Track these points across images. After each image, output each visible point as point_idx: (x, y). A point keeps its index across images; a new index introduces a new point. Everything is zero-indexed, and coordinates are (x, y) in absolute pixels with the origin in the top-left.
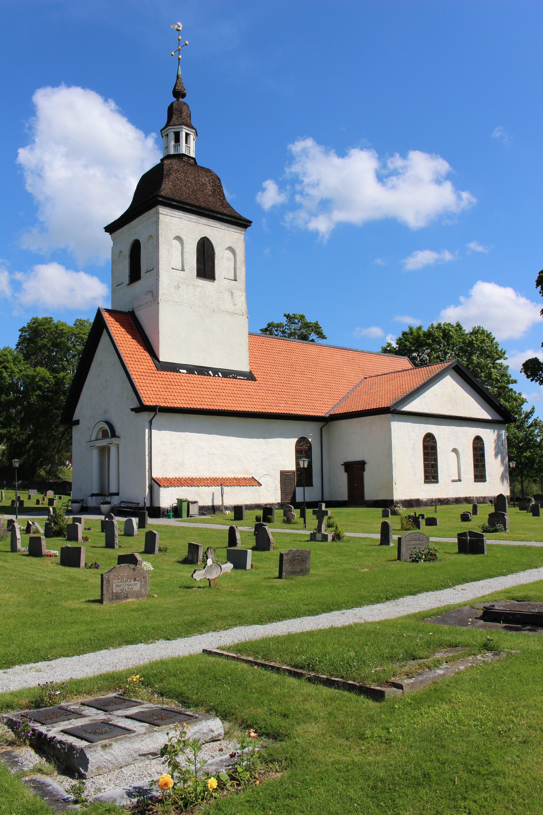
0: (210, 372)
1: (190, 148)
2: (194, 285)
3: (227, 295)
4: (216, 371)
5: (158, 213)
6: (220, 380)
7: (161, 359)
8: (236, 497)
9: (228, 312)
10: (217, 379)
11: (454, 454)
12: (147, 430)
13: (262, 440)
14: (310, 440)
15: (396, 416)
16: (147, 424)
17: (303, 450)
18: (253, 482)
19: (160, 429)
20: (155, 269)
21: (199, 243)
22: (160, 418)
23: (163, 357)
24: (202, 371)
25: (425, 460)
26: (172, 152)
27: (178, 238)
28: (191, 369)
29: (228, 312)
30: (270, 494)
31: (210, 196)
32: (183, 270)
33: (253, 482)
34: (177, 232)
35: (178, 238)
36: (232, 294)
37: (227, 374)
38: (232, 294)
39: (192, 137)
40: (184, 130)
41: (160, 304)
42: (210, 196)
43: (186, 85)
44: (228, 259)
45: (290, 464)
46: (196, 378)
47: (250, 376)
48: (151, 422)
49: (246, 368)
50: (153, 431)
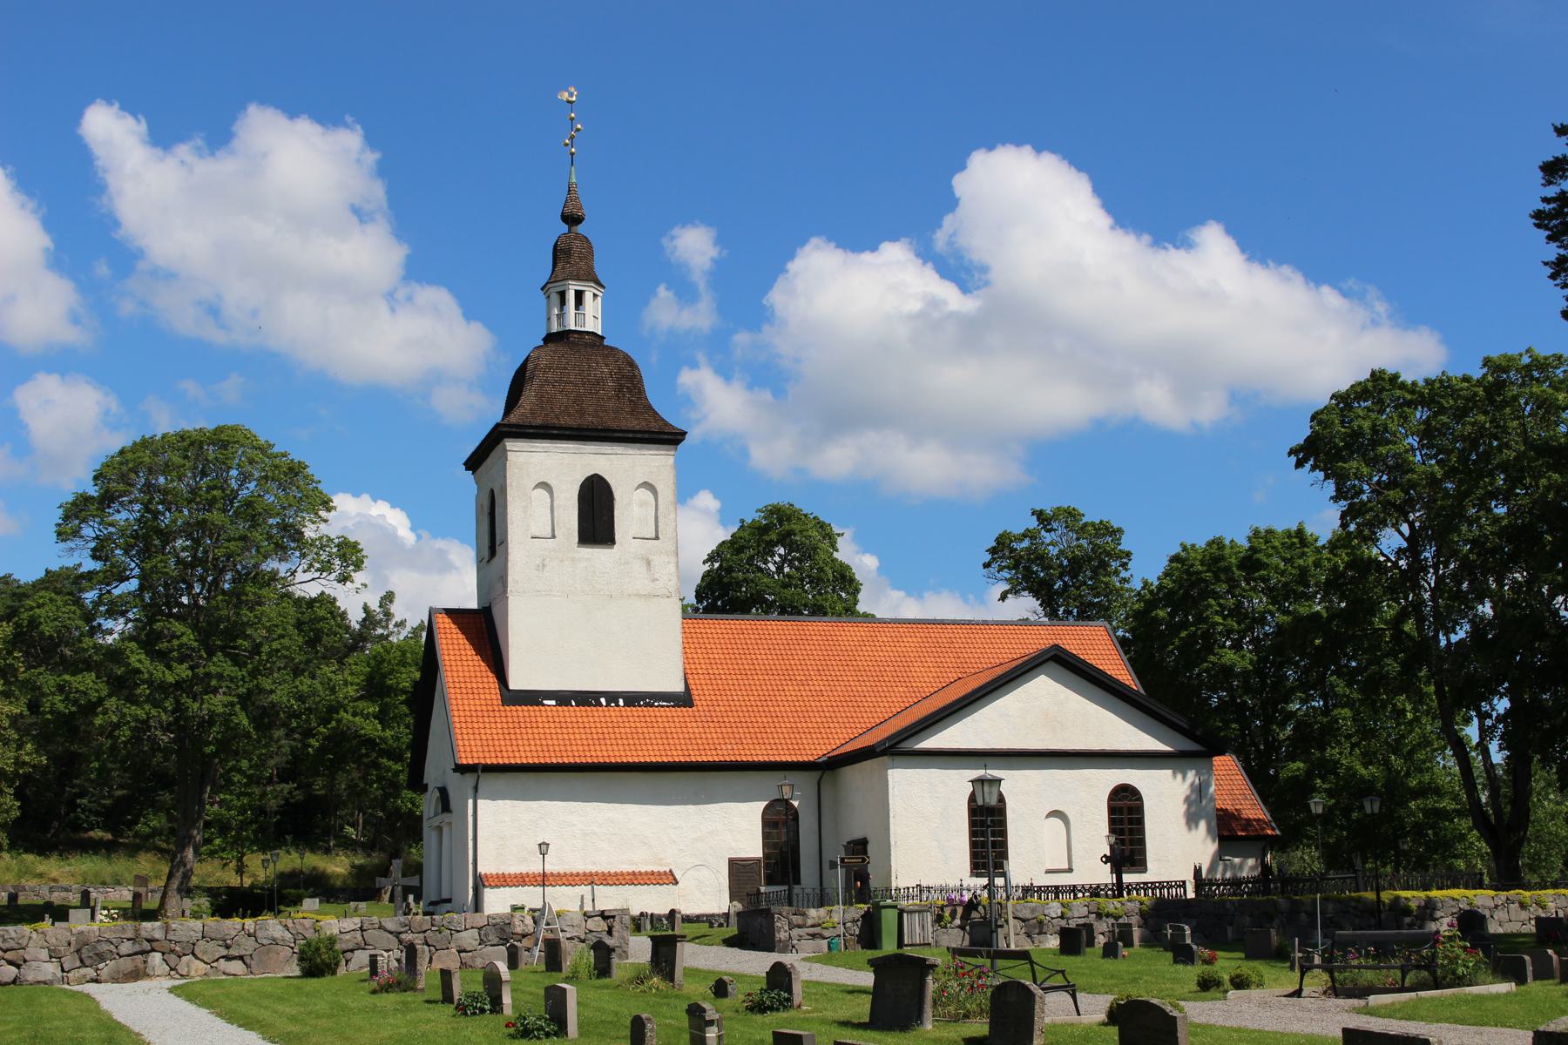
0: (603, 700)
1: (591, 317)
2: (573, 559)
3: (638, 567)
4: (612, 697)
5: (505, 451)
6: (620, 710)
7: (512, 686)
8: (653, 901)
9: (638, 595)
10: (613, 711)
11: (1057, 822)
12: (470, 802)
13: (691, 808)
14: (796, 804)
15: (898, 759)
16: (471, 792)
17: (780, 822)
18: (670, 878)
19: (494, 796)
20: (504, 542)
21: (582, 486)
22: (487, 781)
23: (513, 685)
24: (586, 699)
25: (973, 834)
26: (555, 328)
27: (544, 485)
28: (563, 698)
29: (638, 595)
30: (706, 893)
31: (610, 398)
32: (554, 537)
33: (670, 878)
34: (544, 475)
35: (544, 485)
36: (649, 563)
37: (633, 699)
38: (649, 563)
39: (588, 296)
40: (572, 288)
41: (511, 598)
42: (610, 398)
43: (584, 201)
44: (643, 504)
45: (752, 846)
46: (573, 711)
47: (683, 700)
48: (476, 789)
49: (678, 687)
50: (479, 802)
